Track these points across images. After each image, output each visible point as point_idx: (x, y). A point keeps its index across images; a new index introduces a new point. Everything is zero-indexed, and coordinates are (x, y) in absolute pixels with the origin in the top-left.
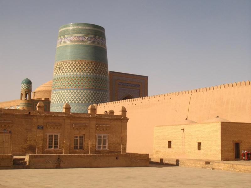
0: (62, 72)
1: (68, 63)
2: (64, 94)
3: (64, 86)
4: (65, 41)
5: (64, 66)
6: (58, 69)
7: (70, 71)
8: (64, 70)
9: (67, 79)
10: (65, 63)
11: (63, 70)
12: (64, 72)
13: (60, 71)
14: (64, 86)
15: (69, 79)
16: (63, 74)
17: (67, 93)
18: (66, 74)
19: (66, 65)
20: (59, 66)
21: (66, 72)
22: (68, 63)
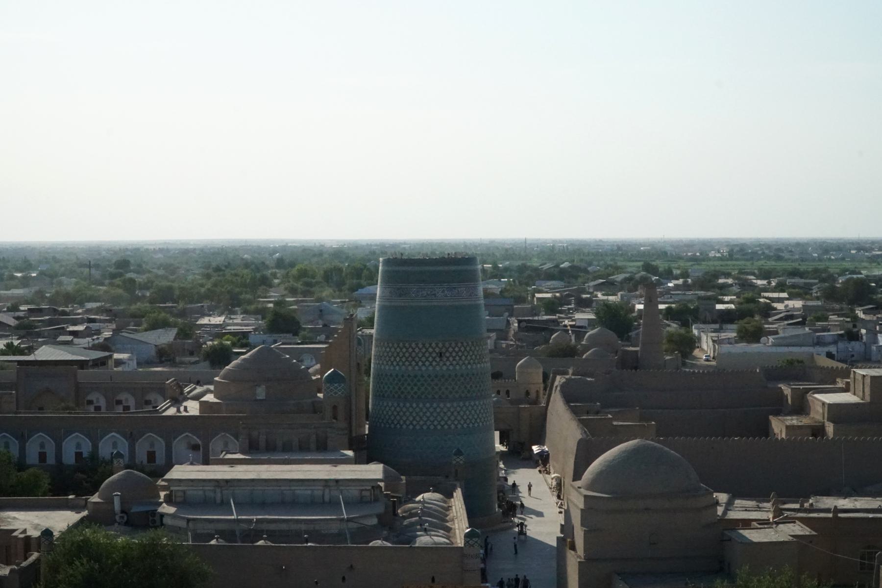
0: (448, 363)
1: (459, 345)
2: (458, 409)
3: (457, 392)
4: (446, 296)
5: (451, 349)
6: (434, 355)
7: (467, 362)
8: (454, 360)
9: (462, 379)
10: (453, 345)
11: (451, 359)
12: (454, 362)
13: (441, 360)
14: (457, 392)
15: (465, 379)
16: (451, 368)
17: (464, 409)
18: (458, 367)
19: (457, 349)
20: (437, 350)
21: (458, 364)
22: (459, 345)
